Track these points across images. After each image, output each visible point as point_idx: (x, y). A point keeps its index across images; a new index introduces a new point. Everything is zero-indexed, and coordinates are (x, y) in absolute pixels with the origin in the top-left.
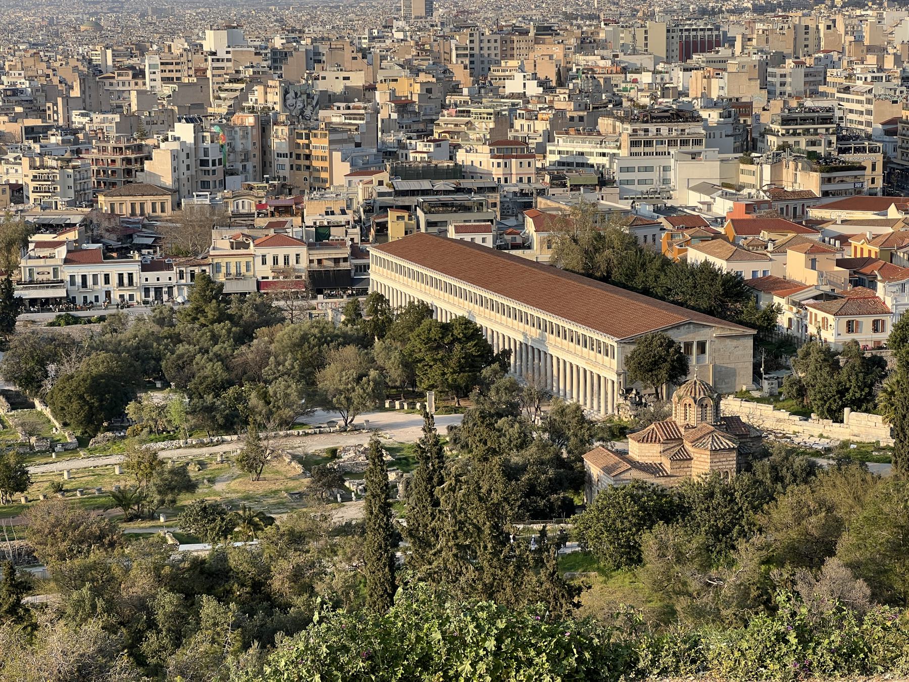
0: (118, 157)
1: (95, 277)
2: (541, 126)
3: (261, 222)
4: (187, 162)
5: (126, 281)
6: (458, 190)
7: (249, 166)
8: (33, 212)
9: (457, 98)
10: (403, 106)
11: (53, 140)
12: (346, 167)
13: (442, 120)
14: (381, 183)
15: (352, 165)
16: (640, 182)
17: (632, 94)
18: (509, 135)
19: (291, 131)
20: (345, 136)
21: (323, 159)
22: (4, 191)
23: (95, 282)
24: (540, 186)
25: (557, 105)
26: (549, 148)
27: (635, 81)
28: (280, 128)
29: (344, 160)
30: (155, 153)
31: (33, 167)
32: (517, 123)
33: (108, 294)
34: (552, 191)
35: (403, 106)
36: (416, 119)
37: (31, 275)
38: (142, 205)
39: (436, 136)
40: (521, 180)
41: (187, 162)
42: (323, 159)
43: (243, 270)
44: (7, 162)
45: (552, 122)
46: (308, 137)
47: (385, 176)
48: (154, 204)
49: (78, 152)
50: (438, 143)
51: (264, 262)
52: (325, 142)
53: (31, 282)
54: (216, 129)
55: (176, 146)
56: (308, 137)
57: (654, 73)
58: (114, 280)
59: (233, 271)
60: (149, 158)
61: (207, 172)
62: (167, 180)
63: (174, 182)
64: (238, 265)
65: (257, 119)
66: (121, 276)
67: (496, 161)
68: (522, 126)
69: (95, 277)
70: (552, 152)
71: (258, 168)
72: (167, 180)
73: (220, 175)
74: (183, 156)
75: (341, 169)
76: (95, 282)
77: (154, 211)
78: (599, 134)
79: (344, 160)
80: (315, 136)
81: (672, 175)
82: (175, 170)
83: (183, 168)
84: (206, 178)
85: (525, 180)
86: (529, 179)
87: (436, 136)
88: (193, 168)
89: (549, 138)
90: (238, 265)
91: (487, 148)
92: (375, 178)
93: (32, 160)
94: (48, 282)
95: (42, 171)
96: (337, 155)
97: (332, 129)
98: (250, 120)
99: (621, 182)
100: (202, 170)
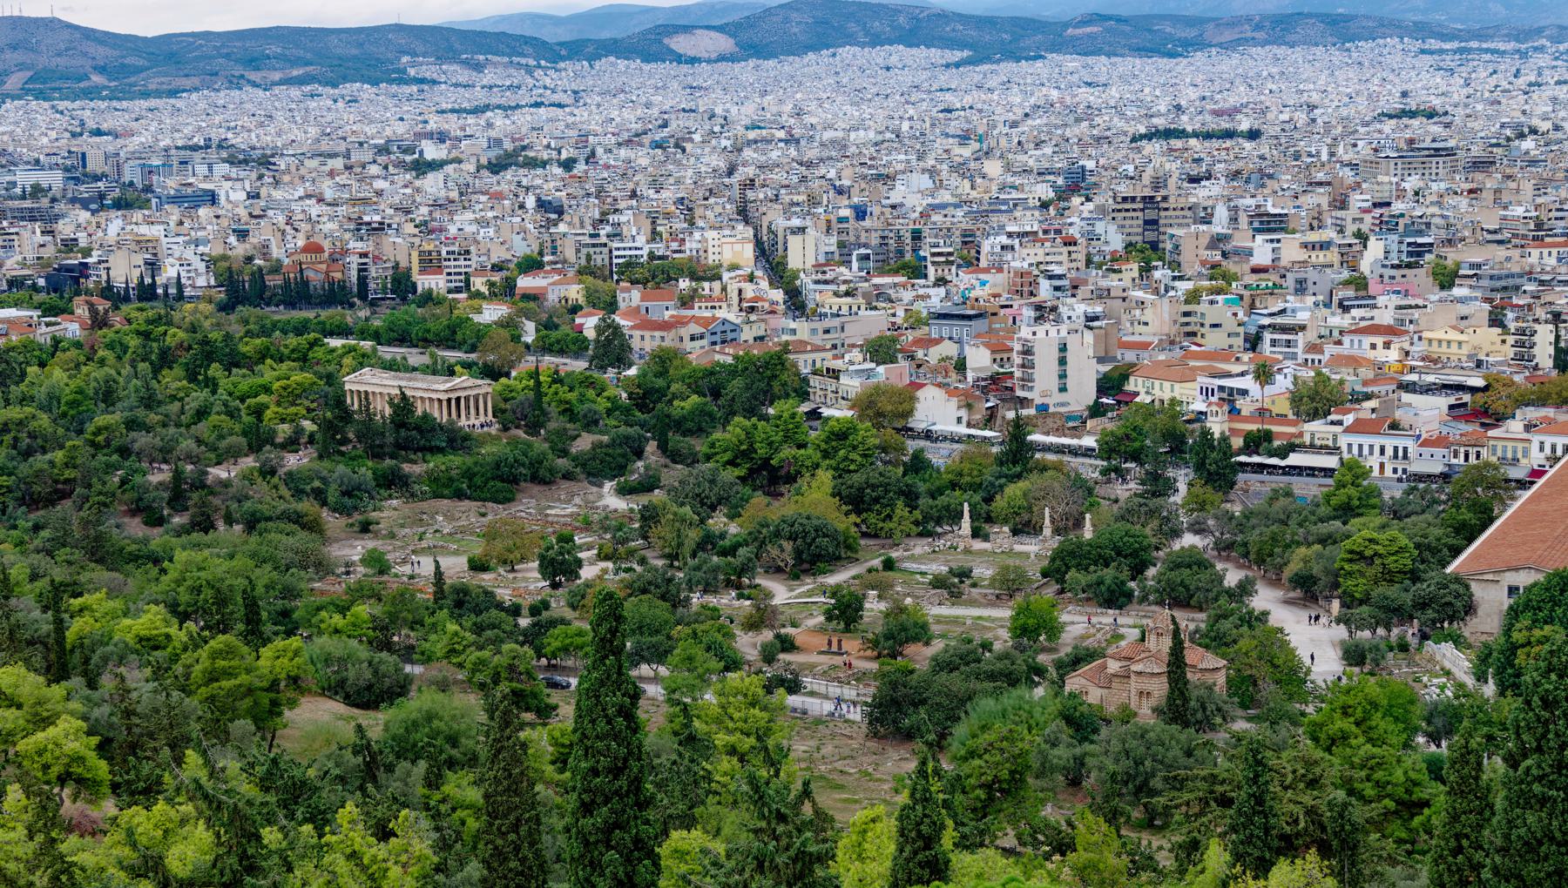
1: (1371, 447)
5: (1401, 454)
23: (1371, 453)
33: (1382, 466)
37: (1312, 439)
43: (1519, 455)
51: (1542, 449)
53: (1312, 446)
58: (1389, 452)
59: (1510, 455)
64: (1515, 452)
66: (1396, 448)
69: (1371, 447)
76: (1371, 453)
90: (1515, 452)
94: (1327, 447)
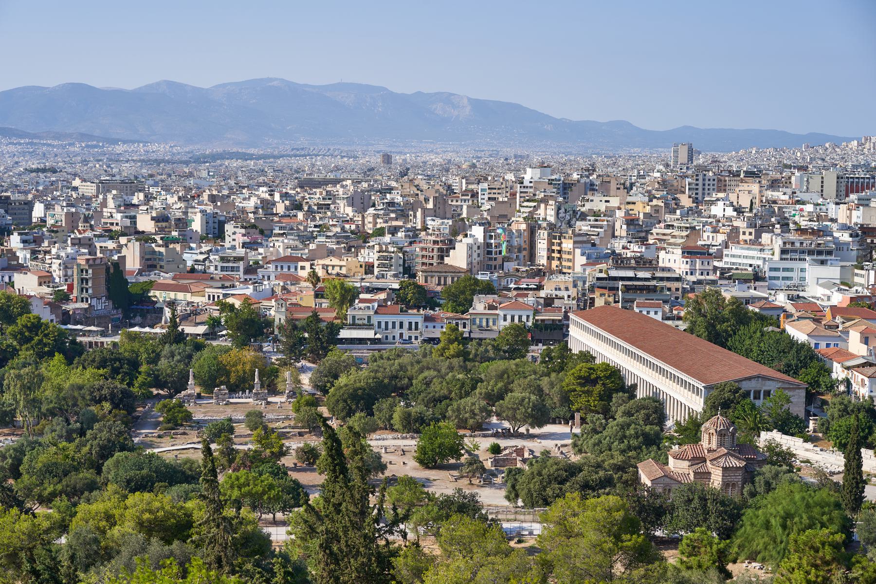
2: (721, 238)
4: (478, 251)
6: (654, 278)
7: (521, 256)
12: (583, 260)
13: (654, 231)
14: (601, 271)
15: (587, 259)
16: (784, 278)
17: (797, 219)
19: (549, 235)
20: (585, 239)
21: (569, 253)
22: (361, 266)
25: (735, 224)
26: (724, 253)
27: (802, 210)
28: (542, 232)
29: (583, 254)
30: (457, 245)
32: (705, 235)
34: (720, 282)
35: (631, 222)
39: (651, 242)
41: (478, 251)
42: (569, 253)
45: (729, 236)
46: (560, 239)
54: (499, 231)
55: (469, 240)
56: (560, 239)
57: (814, 205)
60: (454, 248)
61: (491, 259)
63: (468, 264)
67: (685, 260)
68: (708, 237)
70: (727, 255)
71: (527, 258)
73: (499, 261)
74: (475, 248)
75: (580, 260)
78: (760, 244)
79: (583, 254)
80: (565, 238)
81: (807, 275)
82: (470, 256)
83: (475, 255)
84: (490, 263)
95: (384, 254)
96: (578, 252)
99: (771, 278)
100: (487, 256)
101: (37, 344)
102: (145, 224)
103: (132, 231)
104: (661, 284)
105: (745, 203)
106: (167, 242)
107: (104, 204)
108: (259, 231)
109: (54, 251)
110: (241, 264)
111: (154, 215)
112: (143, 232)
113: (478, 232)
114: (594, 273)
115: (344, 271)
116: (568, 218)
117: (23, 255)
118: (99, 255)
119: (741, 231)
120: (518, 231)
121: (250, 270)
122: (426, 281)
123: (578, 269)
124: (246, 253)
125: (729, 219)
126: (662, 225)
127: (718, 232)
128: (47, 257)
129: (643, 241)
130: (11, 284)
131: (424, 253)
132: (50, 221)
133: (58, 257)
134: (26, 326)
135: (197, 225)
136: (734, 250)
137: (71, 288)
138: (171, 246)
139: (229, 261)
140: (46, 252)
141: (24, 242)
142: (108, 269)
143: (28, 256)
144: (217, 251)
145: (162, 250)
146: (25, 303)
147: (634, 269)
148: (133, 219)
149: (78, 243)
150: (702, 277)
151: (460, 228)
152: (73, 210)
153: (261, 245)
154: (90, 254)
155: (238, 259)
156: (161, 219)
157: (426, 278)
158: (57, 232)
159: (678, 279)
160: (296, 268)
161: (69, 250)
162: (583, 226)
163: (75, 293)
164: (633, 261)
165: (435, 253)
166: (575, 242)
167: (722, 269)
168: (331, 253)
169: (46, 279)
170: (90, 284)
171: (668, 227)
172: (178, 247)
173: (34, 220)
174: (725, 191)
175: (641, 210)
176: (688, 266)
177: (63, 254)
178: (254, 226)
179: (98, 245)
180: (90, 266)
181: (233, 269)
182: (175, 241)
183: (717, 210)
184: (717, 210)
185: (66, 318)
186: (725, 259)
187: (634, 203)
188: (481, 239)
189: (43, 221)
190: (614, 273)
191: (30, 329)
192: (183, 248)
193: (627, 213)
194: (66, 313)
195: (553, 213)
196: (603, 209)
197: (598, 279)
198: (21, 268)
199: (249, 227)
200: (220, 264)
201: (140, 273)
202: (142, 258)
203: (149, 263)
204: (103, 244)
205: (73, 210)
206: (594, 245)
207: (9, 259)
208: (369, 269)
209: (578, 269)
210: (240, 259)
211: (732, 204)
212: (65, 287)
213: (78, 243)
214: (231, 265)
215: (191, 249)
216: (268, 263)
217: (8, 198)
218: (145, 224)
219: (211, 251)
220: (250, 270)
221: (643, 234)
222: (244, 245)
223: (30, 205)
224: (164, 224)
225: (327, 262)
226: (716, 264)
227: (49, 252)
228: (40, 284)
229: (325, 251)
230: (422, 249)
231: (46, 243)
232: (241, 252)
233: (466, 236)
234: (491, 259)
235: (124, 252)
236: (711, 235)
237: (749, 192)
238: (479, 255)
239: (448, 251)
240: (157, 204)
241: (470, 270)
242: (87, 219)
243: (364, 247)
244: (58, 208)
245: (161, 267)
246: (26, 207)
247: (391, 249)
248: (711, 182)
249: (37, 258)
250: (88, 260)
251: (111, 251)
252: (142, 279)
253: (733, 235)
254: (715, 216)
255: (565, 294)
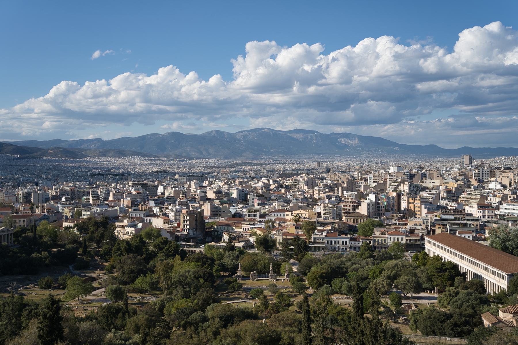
0: (351, 204)
2: (498, 200)
3: (393, 227)
8: (321, 220)
9: (470, 189)
10: (449, 192)
11: (333, 199)
12: (426, 211)
18: (486, 202)
20: (426, 200)
24: (496, 219)
29: (425, 208)
30: (362, 203)
31: (324, 207)
32: (489, 198)
35: (449, 192)
36: (453, 196)
38: (357, 220)
39: (459, 202)
40: (489, 218)
44: (318, 205)
45: (502, 198)
47: (438, 214)
48: (361, 220)
49: (340, 203)
50: (459, 204)
52: (419, 202)
55: (368, 201)
61: (379, 210)
62: (365, 213)
65: (397, 194)
67: (479, 211)
72: (365, 213)
73: (383, 211)
74: (371, 205)
75: (424, 211)
77: (361, 222)
79: (425, 208)
82: (368, 209)
83: (371, 209)
85: (491, 217)
86: (492, 218)
87: (459, 202)
88: (375, 209)
89: (501, 203)
91: (476, 206)
92: (435, 214)
93: (324, 205)
96: (423, 206)
97: (422, 198)
98: (394, 194)
100: (376, 209)
101: (166, 251)
102: (211, 195)
103: (205, 199)
104: (469, 222)
105: (506, 182)
106: (222, 203)
107: (190, 186)
108: (265, 198)
109: (170, 207)
110: (258, 213)
111: (215, 190)
112: (210, 199)
113: (372, 197)
114: (431, 218)
115: (307, 216)
116: (415, 190)
117: (156, 210)
118: (191, 209)
119: (509, 196)
120: (392, 197)
121: (262, 216)
122: (347, 221)
123: (423, 215)
124: (260, 208)
125: (500, 190)
126: (466, 193)
127: (496, 196)
128: (167, 210)
129: (456, 201)
130: (151, 223)
131: (346, 208)
132: (167, 194)
133: (172, 211)
134: (161, 242)
135: (235, 195)
136: (505, 205)
137: (179, 225)
138: (224, 205)
139: (251, 212)
140: (166, 208)
141: (155, 203)
142: (197, 215)
143: (158, 210)
144: (246, 207)
145: (221, 206)
146: (159, 230)
147: (453, 215)
148: (205, 192)
149: (181, 204)
150: (489, 219)
151: (362, 196)
152: (177, 189)
153: (266, 204)
154: (187, 208)
155: (256, 211)
156: (218, 192)
157: (347, 220)
158: (171, 199)
159: (477, 220)
160: (284, 215)
161: (177, 207)
162: (425, 194)
163: (182, 227)
164: (452, 211)
165: (351, 208)
166: (421, 202)
167: (500, 215)
168: (300, 208)
169: (167, 221)
170: (188, 223)
171: (469, 194)
172: (227, 205)
173: (158, 194)
174: (494, 177)
175: (453, 186)
176: (481, 214)
177: (174, 209)
178: (262, 195)
179: (190, 205)
180: (188, 214)
181: (254, 216)
182: (226, 203)
183: (492, 186)
184: (492, 186)
185: (178, 239)
186: (501, 210)
187: (448, 183)
188: (374, 200)
189: (163, 194)
190: (444, 217)
191: (162, 244)
192: (230, 206)
193: (446, 188)
194: (177, 236)
195: (407, 188)
196: (432, 186)
197: (436, 220)
198: (155, 216)
199: (260, 196)
200: (248, 214)
201: (210, 218)
202: (211, 210)
203: (215, 213)
204: (193, 205)
205: (177, 189)
206: (431, 203)
207: (150, 211)
208: (319, 215)
209: (423, 215)
210: (257, 211)
211: (500, 183)
212: (176, 225)
213: (181, 204)
214: (253, 214)
215: (234, 206)
216: (271, 212)
217: (146, 184)
218: (211, 195)
219: (243, 207)
220: (262, 216)
221: (455, 198)
222: (259, 204)
223: (156, 187)
224: (219, 195)
225: (299, 212)
226: (496, 212)
227: (168, 208)
228: (164, 223)
229: (297, 207)
230: (345, 206)
231: (166, 204)
232: (257, 207)
233: (366, 199)
234: (379, 210)
235: (203, 208)
236: (492, 198)
237: (508, 177)
238: (373, 208)
239: (357, 207)
240: (215, 186)
241: (369, 216)
242: (184, 193)
243: (315, 205)
244: (169, 188)
245: (220, 215)
246: (155, 188)
247: (330, 205)
248: (487, 173)
249: (162, 211)
250: (187, 212)
251: (196, 207)
252: (211, 221)
253: (505, 198)
254: (492, 189)
255: (420, 227)
